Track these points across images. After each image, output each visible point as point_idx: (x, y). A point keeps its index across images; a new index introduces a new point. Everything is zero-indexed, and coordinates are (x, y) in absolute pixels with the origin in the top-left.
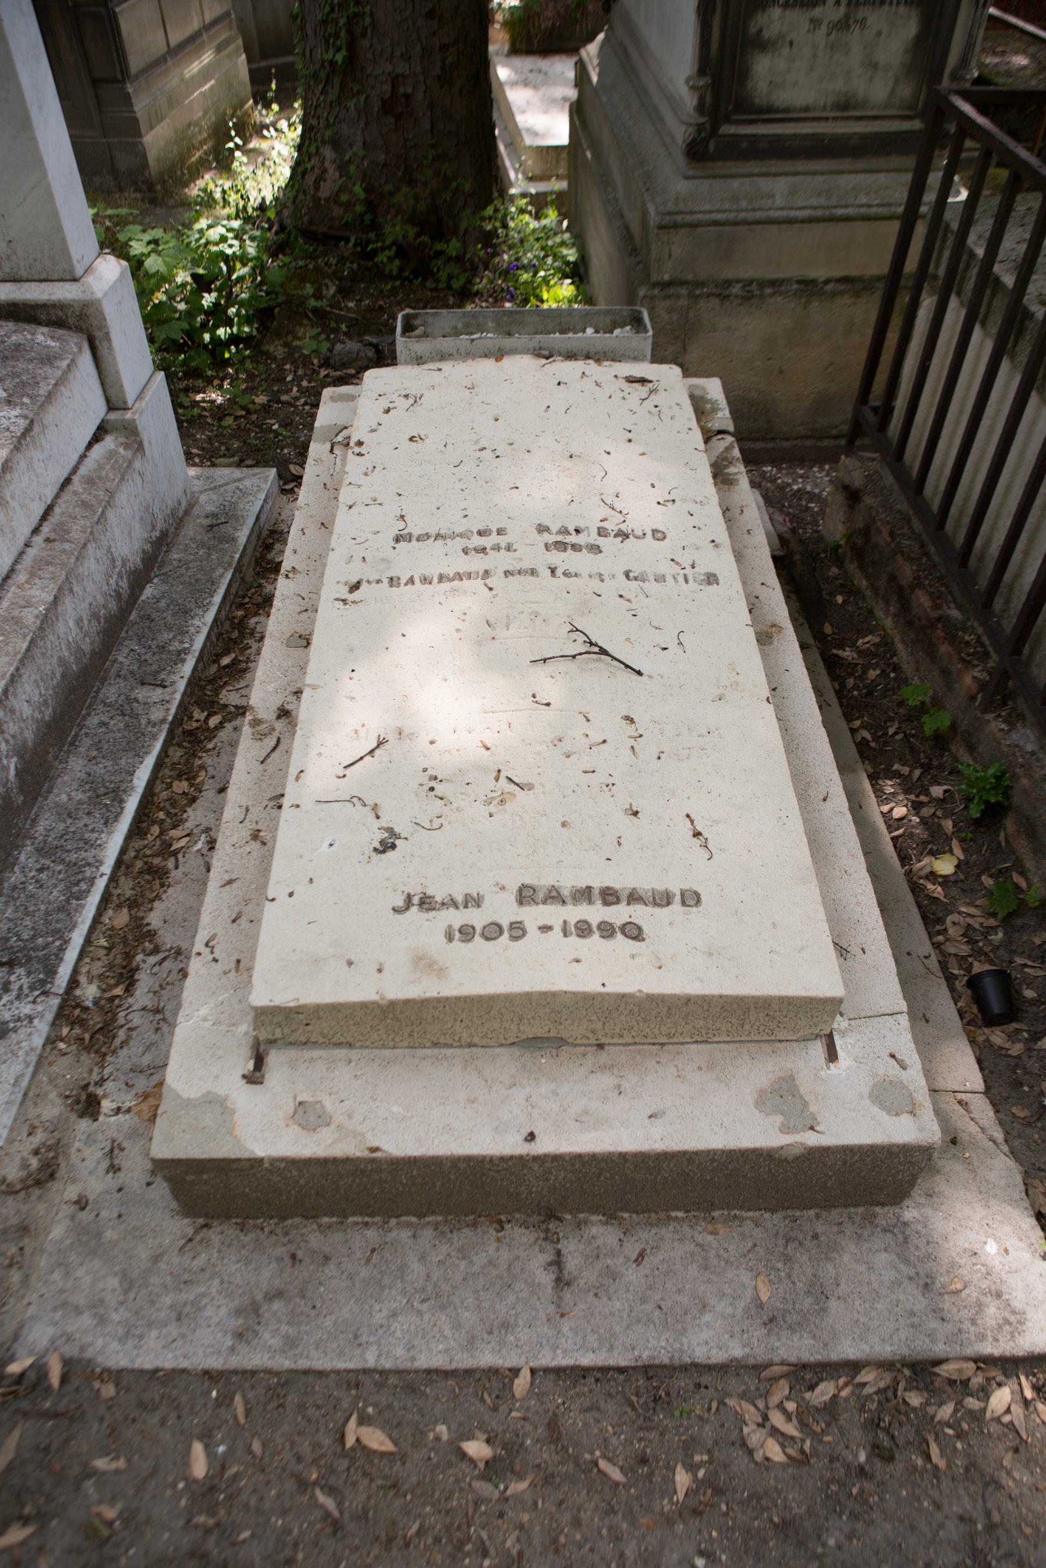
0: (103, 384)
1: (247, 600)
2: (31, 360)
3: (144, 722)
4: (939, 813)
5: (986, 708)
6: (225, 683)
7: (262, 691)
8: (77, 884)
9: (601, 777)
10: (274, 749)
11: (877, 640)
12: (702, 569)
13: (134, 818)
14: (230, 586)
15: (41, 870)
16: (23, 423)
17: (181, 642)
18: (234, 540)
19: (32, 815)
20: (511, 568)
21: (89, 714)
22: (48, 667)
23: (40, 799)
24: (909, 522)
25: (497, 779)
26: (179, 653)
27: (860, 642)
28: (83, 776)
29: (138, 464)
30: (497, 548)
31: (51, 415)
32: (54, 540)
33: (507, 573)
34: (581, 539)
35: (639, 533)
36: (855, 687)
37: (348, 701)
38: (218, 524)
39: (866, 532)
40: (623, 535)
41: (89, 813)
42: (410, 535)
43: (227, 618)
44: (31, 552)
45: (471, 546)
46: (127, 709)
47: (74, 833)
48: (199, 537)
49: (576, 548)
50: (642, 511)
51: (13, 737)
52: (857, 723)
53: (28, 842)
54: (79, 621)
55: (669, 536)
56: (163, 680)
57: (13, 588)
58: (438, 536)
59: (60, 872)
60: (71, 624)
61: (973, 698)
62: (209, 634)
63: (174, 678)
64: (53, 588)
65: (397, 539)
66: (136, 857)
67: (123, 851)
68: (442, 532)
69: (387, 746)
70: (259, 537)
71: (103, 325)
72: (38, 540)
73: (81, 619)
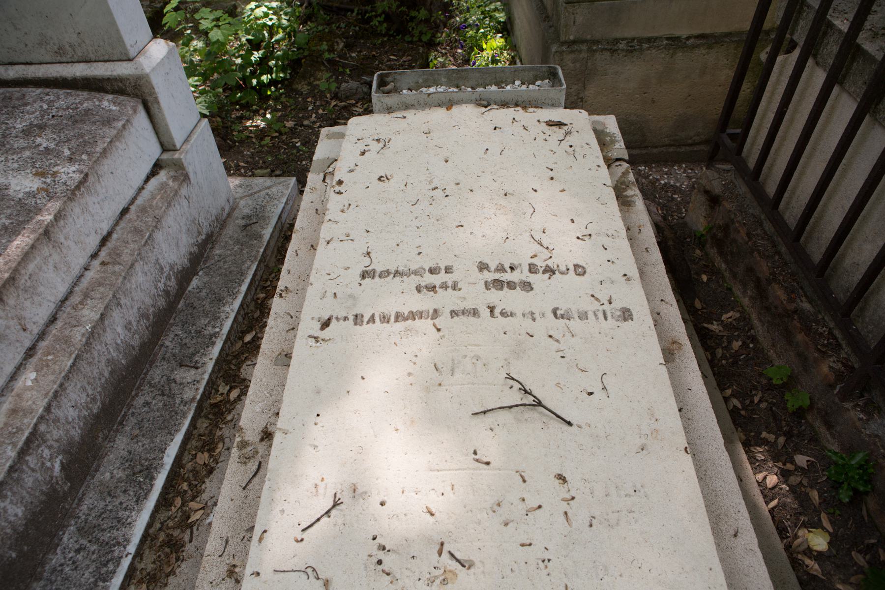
0: (157, 133)
1: (269, 283)
2: (94, 123)
3: (178, 401)
4: (805, 482)
5: (845, 396)
6: (246, 358)
7: (250, 415)
8: (105, 565)
9: (536, 552)
10: (254, 476)
11: (738, 315)
12: (618, 305)
13: (161, 494)
14: (255, 275)
15: (78, 551)
16: (78, 177)
17: (214, 327)
18: (260, 237)
19: (80, 494)
20: (456, 308)
21: (137, 395)
22: (96, 371)
23: (88, 478)
24: (761, 225)
25: (440, 553)
26: (211, 336)
27: (724, 317)
28: (125, 454)
29: (184, 191)
30: (444, 286)
31: (106, 165)
32: (108, 263)
33: (454, 313)
34: (514, 277)
35: (563, 269)
36: (723, 357)
37: (311, 449)
38: (251, 223)
39: (726, 228)
40: (550, 271)
41: (125, 491)
42: (374, 271)
43: (253, 299)
44: (89, 275)
45: (423, 284)
46: (167, 390)
47: (111, 511)
48: (236, 235)
49: (511, 285)
50: (567, 250)
51: (57, 441)
52: (729, 392)
53: (73, 522)
54: (128, 326)
55: (588, 271)
56: (197, 362)
57: (69, 309)
58: (397, 273)
59: (93, 553)
60: (119, 330)
61: (832, 386)
62: (236, 317)
63: (206, 359)
64: (101, 307)
65: (363, 276)
66: (160, 529)
67: (149, 525)
68: (400, 269)
69: (342, 507)
70: (281, 231)
71: (152, 92)
72: (96, 263)
73: (130, 323)
